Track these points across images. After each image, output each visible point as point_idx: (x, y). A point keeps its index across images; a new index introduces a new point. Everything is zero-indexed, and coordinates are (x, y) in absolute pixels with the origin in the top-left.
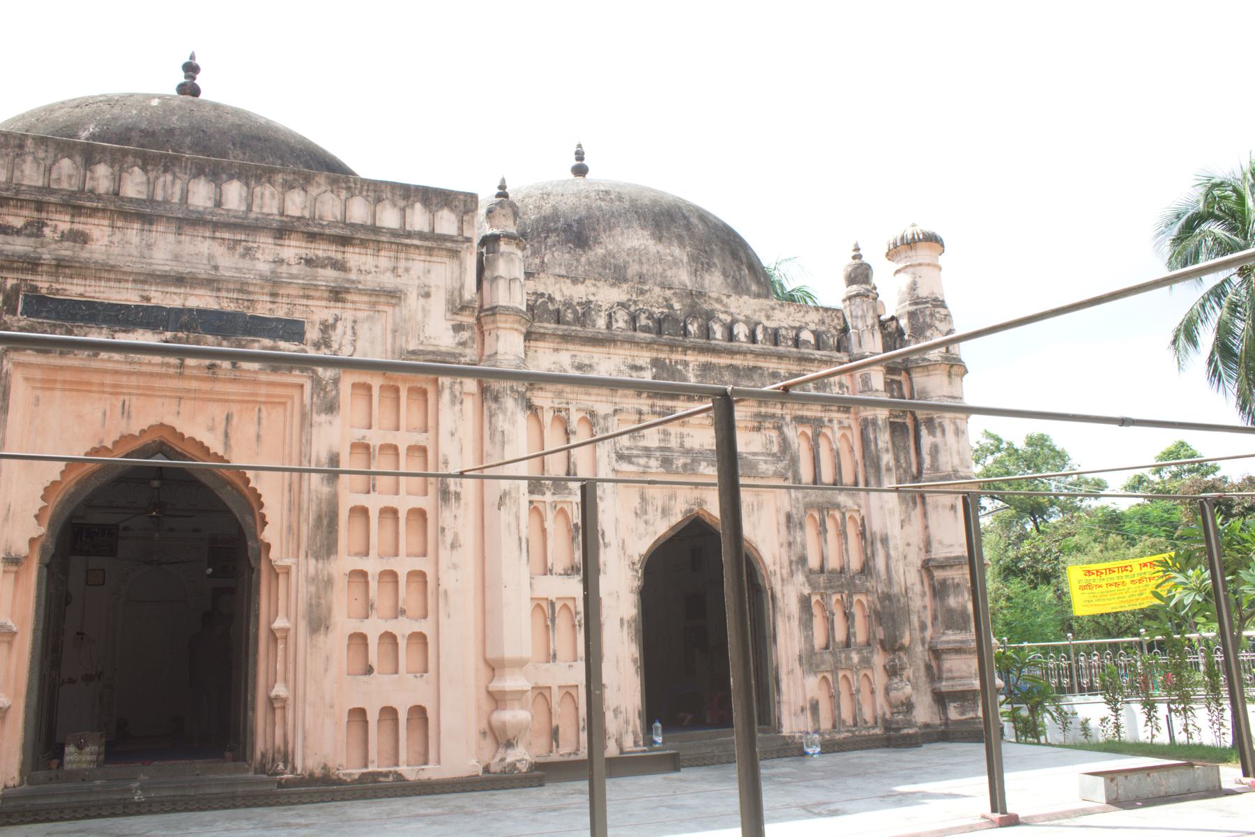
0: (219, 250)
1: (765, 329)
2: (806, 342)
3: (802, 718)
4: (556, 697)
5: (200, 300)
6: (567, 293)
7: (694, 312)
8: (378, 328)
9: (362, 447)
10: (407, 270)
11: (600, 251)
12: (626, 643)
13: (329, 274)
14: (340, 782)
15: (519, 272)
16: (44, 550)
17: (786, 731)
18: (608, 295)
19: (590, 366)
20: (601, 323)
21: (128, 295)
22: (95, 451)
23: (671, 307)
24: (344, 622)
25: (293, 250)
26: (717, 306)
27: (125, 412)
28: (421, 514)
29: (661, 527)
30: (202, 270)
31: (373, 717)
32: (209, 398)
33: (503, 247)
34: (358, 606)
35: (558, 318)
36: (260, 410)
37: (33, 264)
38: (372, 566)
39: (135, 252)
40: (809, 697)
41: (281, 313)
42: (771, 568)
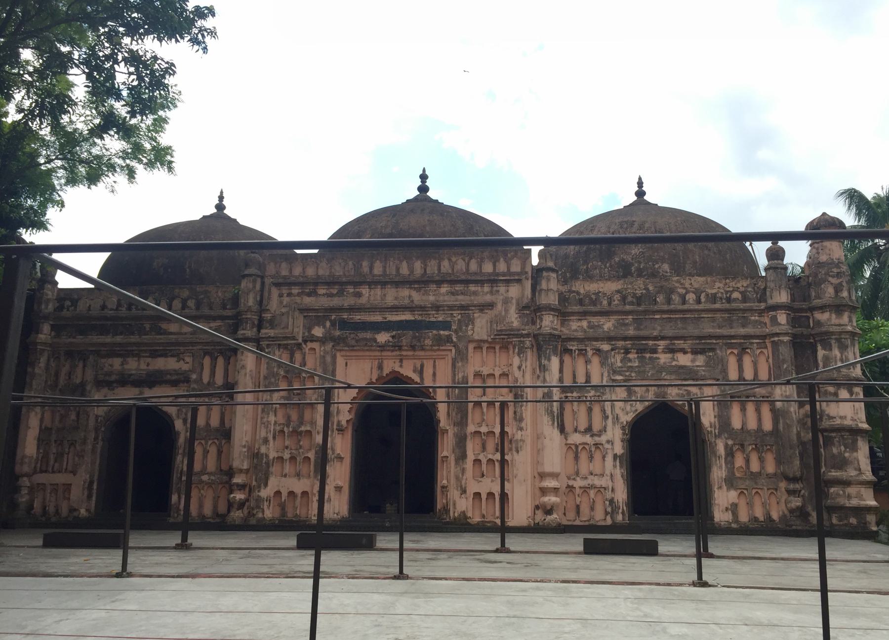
0: (414, 294)
1: (707, 295)
2: (735, 300)
3: (726, 514)
4: (578, 491)
5: (407, 316)
6: (587, 288)
7: (661, 290)
8: (484, 321)
9: (477, 375)
10: (498, 291)
11: (617, 259)
12: (618, 467)
13: (460, 297)
14: (469, 524)
15: (553, 285)
16: (353, 424)
17: (717, 519)
18: (611, 287)
19: (598, 326)
20: (605, 302)
21: (377, 318)
22: (368, 384)
23: (647, 289)
24: (471, 457)
25: (444, 289)
26: (677, 285)
27: (380, 367)
28: (504, 405)
29: (640, 407)
30: (407, 301)
31: (484, 496)
32: (414, 357)
33: (545, 274)
34: (478, 448)
35: (581, 302)
36: (435, 362)
37: (340, 309)
38: (484, 429)
39: (379, 298)
40: (730, 502)
41: (440, 319)
42: (709, 429)
